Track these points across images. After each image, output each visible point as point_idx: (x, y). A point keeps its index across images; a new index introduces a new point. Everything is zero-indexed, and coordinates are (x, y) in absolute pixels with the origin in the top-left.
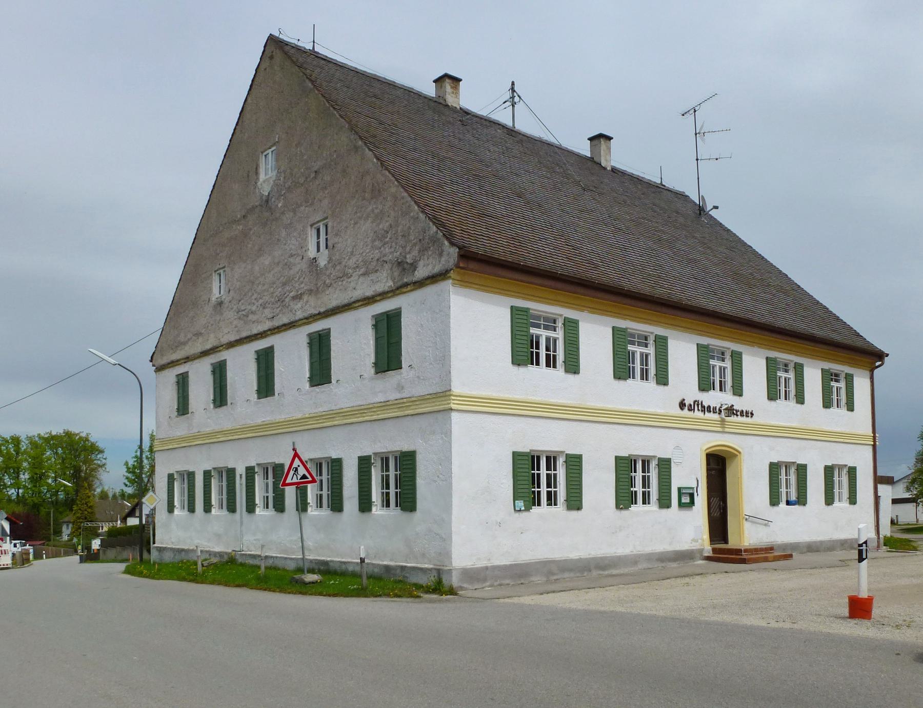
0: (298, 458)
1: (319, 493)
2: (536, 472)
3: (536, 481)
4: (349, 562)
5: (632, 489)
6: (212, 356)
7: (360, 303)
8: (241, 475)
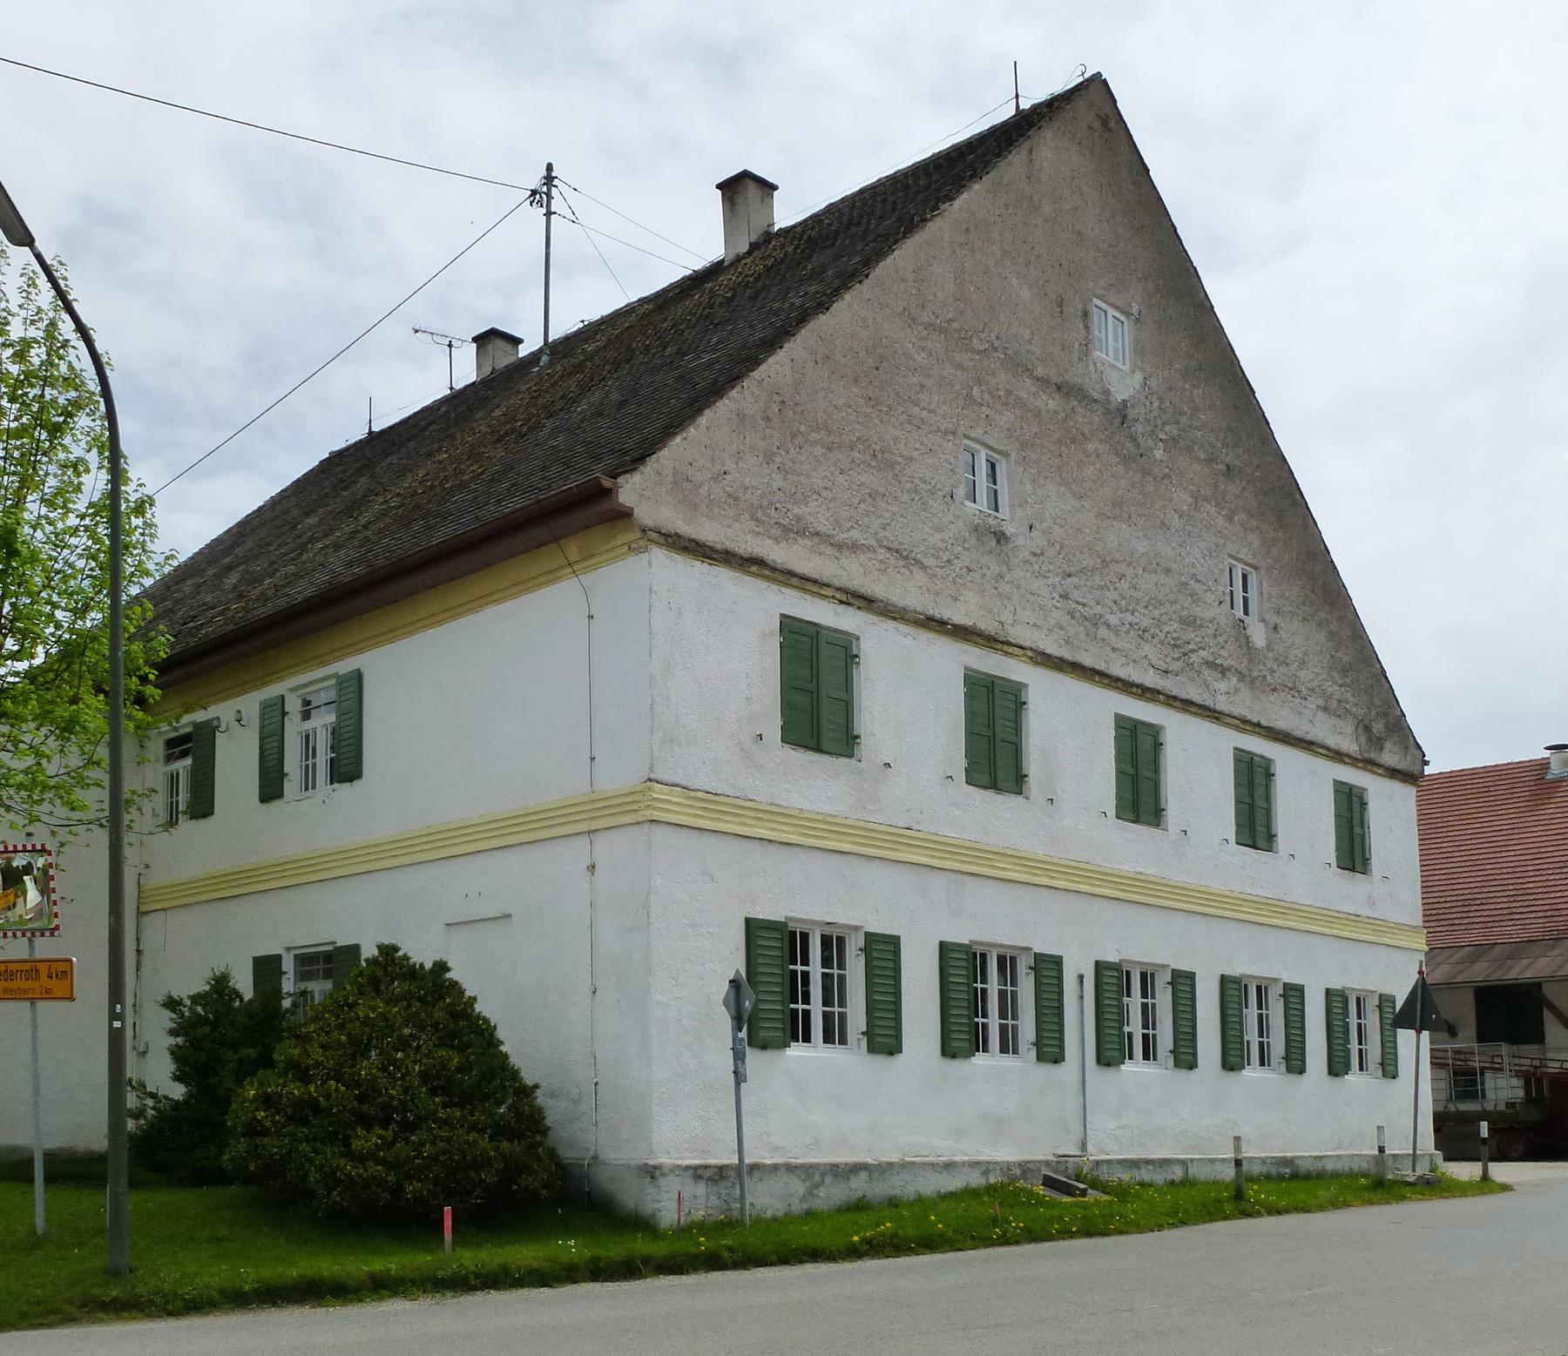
0: (1549, 1008)
1: (1363, 1047)
2: (799, 968)
3: (977, 1002)
4: (1326, 1156)
5: (976, 1020)
6: (978, 651)
7: (1324, 752)
8: (1081, 977)
